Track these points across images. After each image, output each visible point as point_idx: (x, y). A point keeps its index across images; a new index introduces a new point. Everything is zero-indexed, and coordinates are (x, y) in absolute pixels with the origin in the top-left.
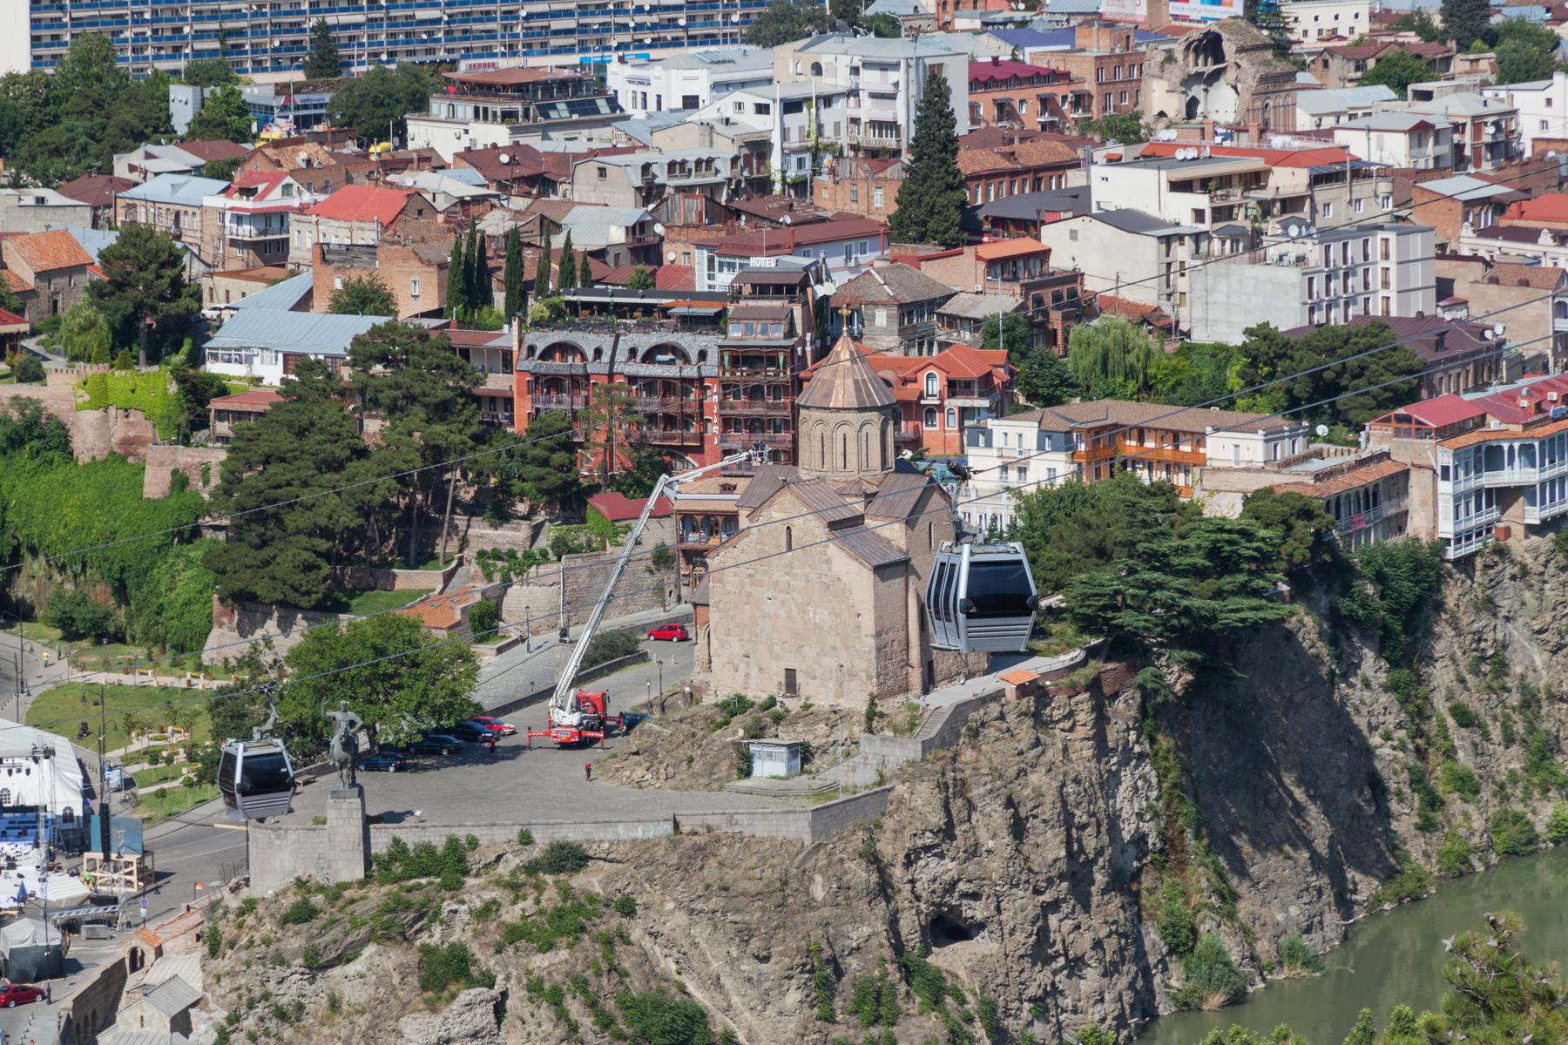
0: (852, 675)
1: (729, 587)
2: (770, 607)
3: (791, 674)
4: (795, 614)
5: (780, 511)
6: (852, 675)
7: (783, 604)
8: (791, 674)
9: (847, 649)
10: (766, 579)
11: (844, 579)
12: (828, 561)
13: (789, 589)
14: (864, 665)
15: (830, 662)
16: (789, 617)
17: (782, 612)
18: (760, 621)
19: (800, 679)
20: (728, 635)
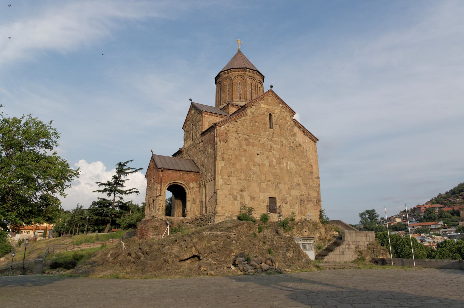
0: (309, 200)
1: (231, 146)
2: (257, 159)
3: (272, 200)
4: (275, 163)
5: (267, 104)
6: (309, 200)
7: (267, 158)
8: (272, 200)
9: (306, 185)
10: (256, 142)
11: (303, 146)
12: (295, 135)
13: (271, 149)
14: (316, 194)
15: (295, 193)
16: (271, 165)
17: (266, 163)
18: (253, 168)
19: (278, 203)
20: (230, 175)
